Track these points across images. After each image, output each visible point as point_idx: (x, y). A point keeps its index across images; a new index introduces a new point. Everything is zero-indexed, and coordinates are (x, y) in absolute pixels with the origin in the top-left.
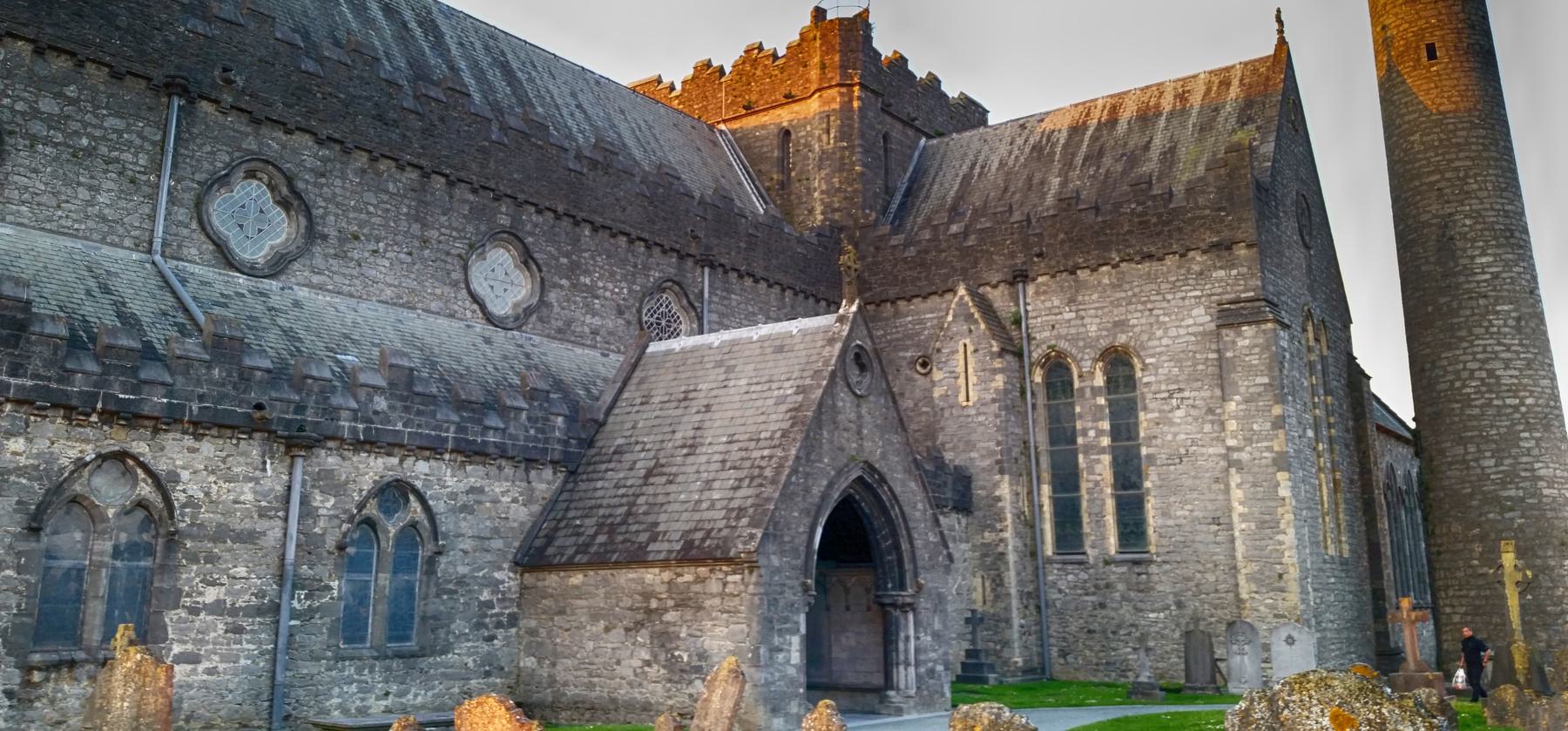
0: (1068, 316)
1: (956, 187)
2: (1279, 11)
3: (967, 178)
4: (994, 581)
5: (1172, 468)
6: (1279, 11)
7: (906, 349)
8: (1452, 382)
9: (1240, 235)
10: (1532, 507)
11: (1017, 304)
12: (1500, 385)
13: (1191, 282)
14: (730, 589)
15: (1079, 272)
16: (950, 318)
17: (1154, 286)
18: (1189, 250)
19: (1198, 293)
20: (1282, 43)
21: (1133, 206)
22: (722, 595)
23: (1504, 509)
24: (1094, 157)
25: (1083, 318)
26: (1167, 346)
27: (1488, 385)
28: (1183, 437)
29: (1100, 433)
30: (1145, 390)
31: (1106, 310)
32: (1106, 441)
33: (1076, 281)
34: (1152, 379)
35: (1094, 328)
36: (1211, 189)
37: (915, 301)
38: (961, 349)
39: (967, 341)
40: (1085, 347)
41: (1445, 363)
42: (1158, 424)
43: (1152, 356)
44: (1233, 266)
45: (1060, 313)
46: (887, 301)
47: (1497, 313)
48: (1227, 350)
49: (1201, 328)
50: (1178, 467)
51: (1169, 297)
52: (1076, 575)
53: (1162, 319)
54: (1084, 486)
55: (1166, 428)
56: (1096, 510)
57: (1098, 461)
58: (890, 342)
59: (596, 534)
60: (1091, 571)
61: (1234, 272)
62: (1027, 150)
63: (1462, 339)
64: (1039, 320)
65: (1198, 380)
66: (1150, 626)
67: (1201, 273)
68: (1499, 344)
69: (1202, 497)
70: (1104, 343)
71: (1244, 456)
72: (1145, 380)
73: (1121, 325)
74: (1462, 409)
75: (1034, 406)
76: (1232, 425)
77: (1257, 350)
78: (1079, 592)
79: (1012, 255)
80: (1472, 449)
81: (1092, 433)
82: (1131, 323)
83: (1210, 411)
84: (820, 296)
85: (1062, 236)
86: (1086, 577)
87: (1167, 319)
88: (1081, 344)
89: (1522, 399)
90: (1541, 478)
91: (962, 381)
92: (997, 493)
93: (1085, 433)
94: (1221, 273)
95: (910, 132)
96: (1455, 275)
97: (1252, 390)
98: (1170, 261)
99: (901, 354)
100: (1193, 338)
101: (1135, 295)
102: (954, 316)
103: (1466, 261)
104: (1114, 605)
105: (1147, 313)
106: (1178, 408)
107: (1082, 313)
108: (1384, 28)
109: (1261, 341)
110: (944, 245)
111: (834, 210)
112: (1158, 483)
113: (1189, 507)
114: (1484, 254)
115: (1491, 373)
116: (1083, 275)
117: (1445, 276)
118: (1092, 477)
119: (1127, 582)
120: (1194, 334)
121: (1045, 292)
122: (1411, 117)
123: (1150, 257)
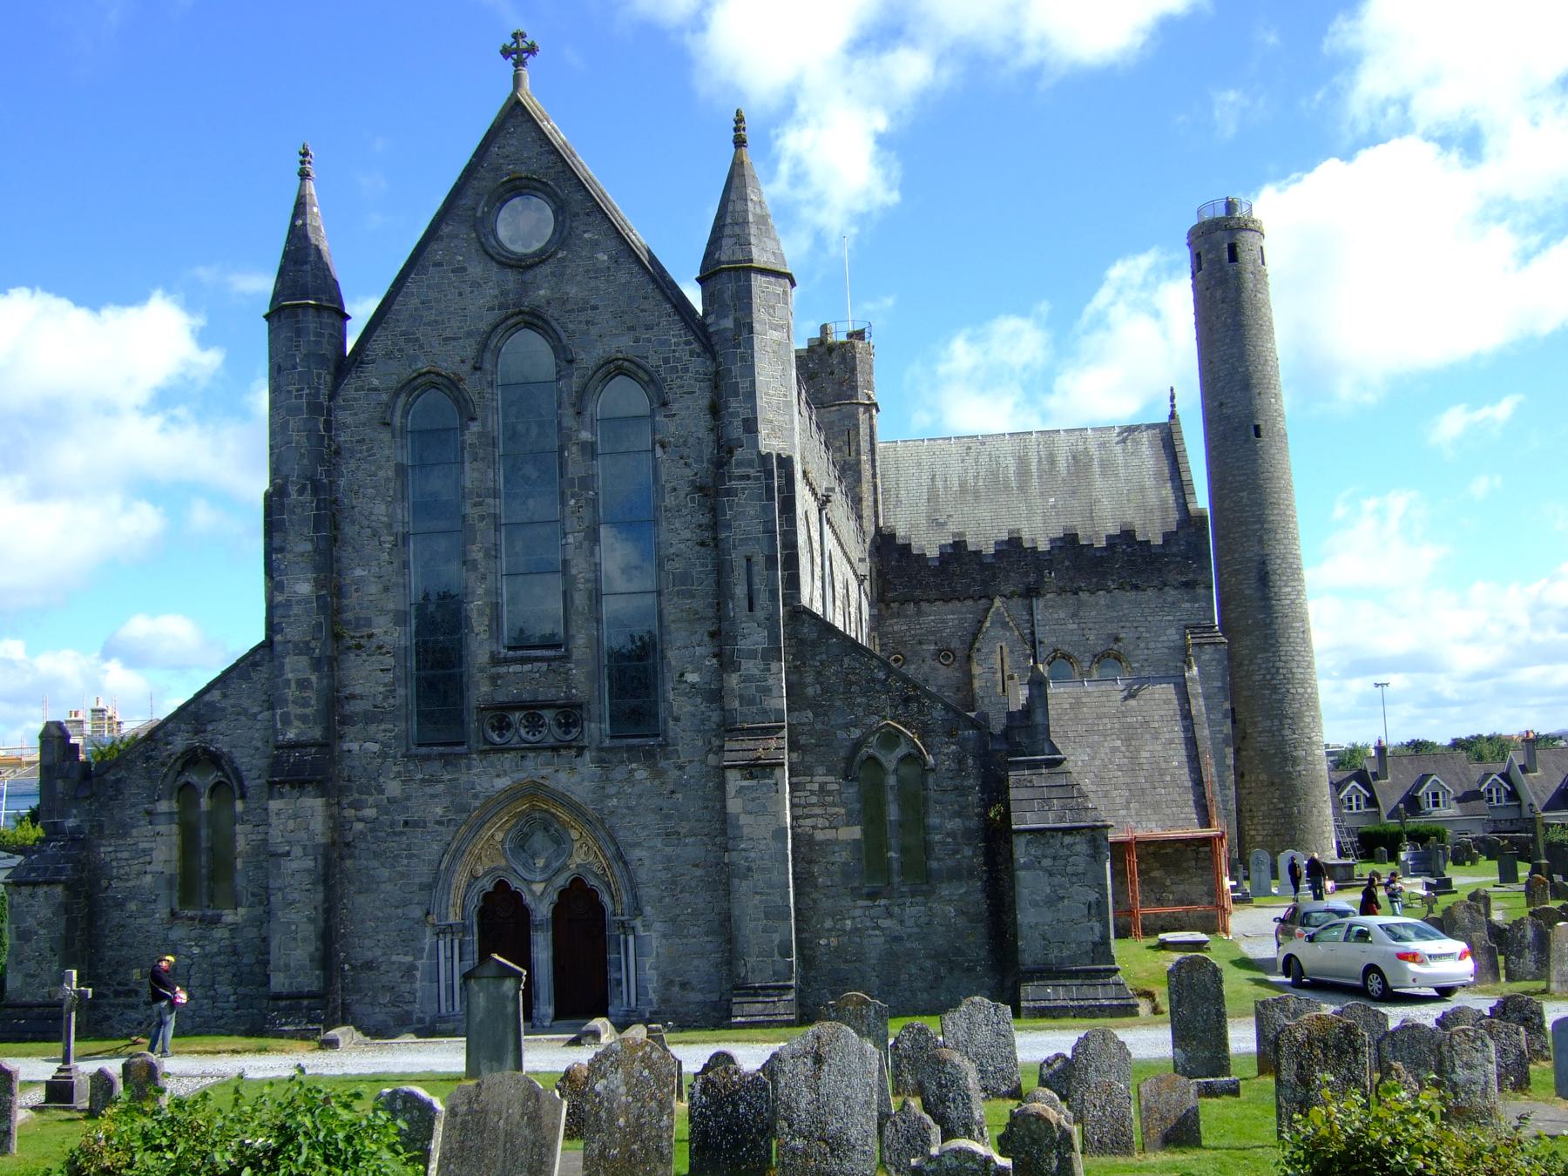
0: (1071, 627)
2: (1172, 390)
6: (1172, 390)
8: (1264, 675)
12: (1293, 678)
15: (1080, 593)
18: (1165, 585)
19: (1171, 618)
20: (1172, 416)
21: (1124, 547)
22: (1197, 860)
25: (1083, 629)
27: (1288, 679)
31: (1102, 625)
36: (1182, 542)
41: (1259, 661)
43: (1138, 662)
44: (1194, 600)
47: (1292, 628)
51: (1149, 619)
61: (1197, 605)
67: (1174, 603)
68: (1295, 650)
70: (1099, 649)
74: (1271, 695)
77: (1214, 663)
79: (1027, 574)
85: (1067, 563)
88: (1082, 649)
89: (1305, 688)
90: (1314, 743)
91: (1000, 675)
94: (1188, 605)
97: (1210, 690)
98: (1150, 592)
99: (925, 647)
101: (1124, 615)
103: (1276, 590)
105: (1133, 629)
107: (1084, 625)
108: (1221, 405)
109: (1217, 656)
114: (1286, 586)
116: (1084, 596)
120: (1169, 648)
121: (1051, 607)
122: (1242, 478)
123: (1136, 587)
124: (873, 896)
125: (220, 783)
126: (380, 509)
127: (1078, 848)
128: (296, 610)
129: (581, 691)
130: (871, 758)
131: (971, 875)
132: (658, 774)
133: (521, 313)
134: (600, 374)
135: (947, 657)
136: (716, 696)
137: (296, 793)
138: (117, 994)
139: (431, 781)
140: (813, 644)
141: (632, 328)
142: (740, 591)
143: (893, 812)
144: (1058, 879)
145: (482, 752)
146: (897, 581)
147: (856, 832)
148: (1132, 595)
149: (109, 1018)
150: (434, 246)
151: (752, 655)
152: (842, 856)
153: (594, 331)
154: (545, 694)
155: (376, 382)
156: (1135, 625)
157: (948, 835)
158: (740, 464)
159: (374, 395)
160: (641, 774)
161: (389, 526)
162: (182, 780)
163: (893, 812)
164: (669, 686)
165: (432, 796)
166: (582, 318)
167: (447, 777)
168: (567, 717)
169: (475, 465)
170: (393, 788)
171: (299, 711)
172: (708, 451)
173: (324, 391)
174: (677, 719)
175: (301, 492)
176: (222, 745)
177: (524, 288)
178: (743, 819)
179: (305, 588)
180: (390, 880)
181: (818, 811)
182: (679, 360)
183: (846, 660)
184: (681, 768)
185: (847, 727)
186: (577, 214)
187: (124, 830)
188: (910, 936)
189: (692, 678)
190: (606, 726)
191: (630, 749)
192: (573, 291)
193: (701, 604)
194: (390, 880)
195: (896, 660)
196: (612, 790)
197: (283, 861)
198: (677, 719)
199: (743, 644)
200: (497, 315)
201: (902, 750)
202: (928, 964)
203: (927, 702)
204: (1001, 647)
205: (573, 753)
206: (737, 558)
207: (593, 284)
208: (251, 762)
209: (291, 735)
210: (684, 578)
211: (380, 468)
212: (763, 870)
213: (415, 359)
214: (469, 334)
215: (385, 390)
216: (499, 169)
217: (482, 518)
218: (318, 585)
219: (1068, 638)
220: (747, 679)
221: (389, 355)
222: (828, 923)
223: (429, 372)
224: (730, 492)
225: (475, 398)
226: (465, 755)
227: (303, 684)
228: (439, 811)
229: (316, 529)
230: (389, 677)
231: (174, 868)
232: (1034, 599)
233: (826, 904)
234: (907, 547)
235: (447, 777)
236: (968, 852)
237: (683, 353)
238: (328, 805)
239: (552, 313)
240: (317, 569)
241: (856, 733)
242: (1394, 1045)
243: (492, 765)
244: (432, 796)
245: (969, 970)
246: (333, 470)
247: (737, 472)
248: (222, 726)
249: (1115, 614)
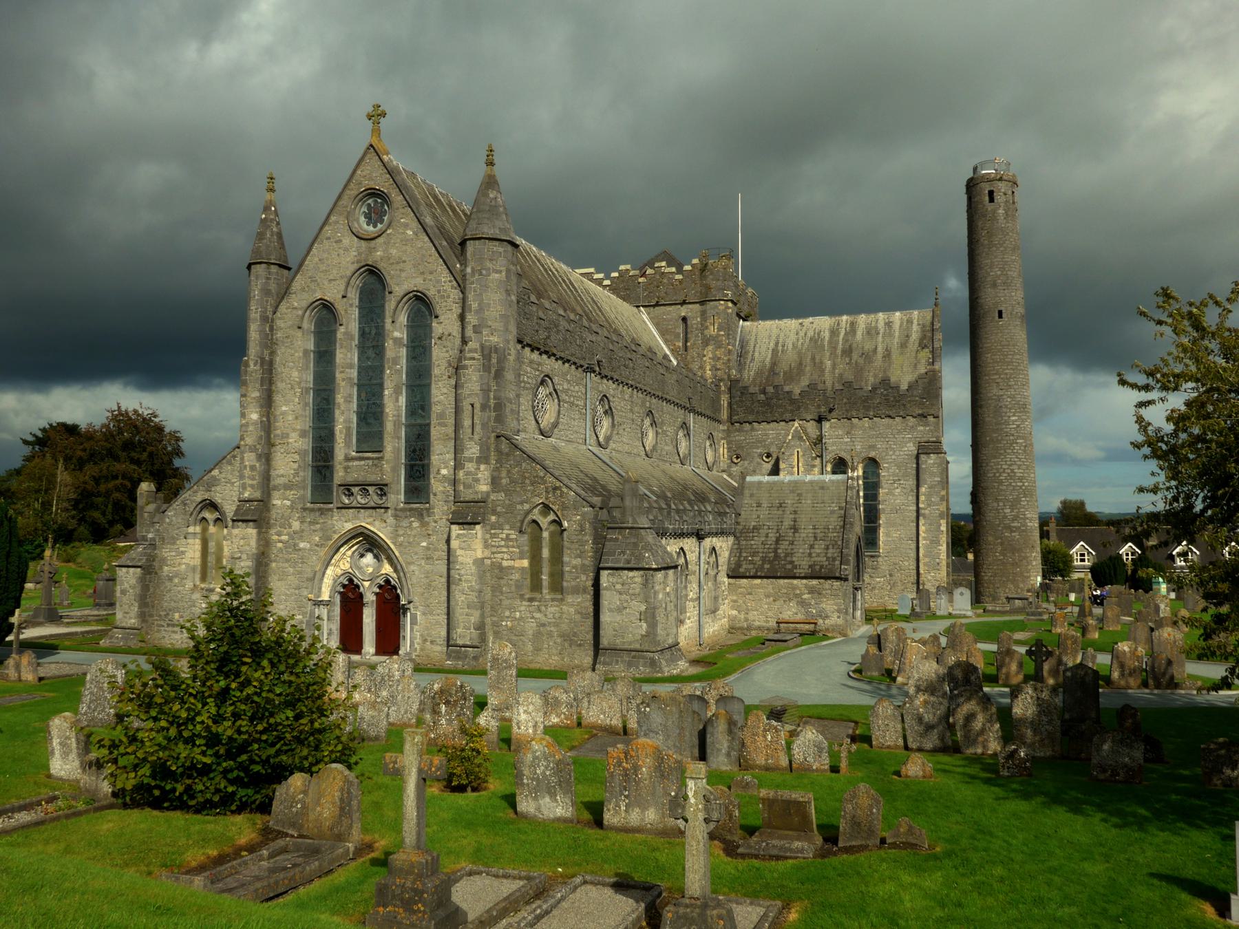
1: (770, 356)
3: (775, 351)
7: (758, 448)
9: (932, 412)
10: (1023, 531)
14: (835, 587)
16: (790, 437)
23: (1012, 531)
24: (848, 352)
44: (927, 425)
58: (748, 443)
59: (763, 564)
62: (807, 341)
63: (1001, 454)
70: (864, 455)
71: (927, 512)
73: (873, 447)
76: (922, 498)
79: (819, 406)
80: (1001, 504)
83: (912, 490)
94: (922, 428)
96: (1000, 424)
98: (898, 419)
110: (781, 397)
111: (717, 369)
115: (1012, 471)
116: (855, 421)
117: (996, 424)
123: (890, 417)
124: (531, 600)
125: (218, 519)
126: (295, 374)
127: (636, 580)
128: (251, 428)
129: (387, 478)
130: (534, 521)
131: (585, 591)
132: (424, 524)
133: (367, 265)
134: (405, 299)
135: (767, 457)
136: (455, 482)
137: (244, 525)
138: (168, 625)
139: (312, 523)
140: (507, 455)
141: (423, 273)
142: (467, 423)
143: (546, 553)
144: (624, 596)
145: (338, 508)
146: (739, 409)
147: (525, 563)
148: (887, 420)
149: (164, 637)
150: (327, 228)
151: (471, 460)
152: (516, 576)
153: (403, 275)
154: (372, 478)
155: (296, 304)
157: (573, 568)
158: (470, 351)
159: (295, 312)
160: (416, 524)
161: (300, 383)
162: (201, 516)
163: (546, 553)
164: (431, 476)
165: (314, 531)
166: (398, 268)
167: (321, 521)
168: (381, 490)
169: (342, 351)
170: (296, 525)
171: (251, 482)
172: (458, 341)
173: (270, 309)
174: (435, 495)
175: (255, 365)
176: (218, 499)
177: (371, 250)
178: (459, 552)
179: (255, 416)
180: (293, 574)
181: (504, 550)
182: (445, 291)
183: (524, 465)
184: (436, 522)
185: (522, 503)
186: (398, 209)
187: (173, 541)
188: (549, 623)
189: (444, 472)
190: (402, 497)
191: (411, 510)
192: (394, 252)
193: (451, 430)
194: (293, 574)
195: (737, 458)
196: (401, 532)
197: (237, 561)
198: (435, 495)
199: (467, 454)
200: (356, 266)
201: (552, 517)
202: (559, 640)
203: (565, 490)
205: (383, 510)
206: (466, 406)
207: (404, 248)
208: (230, 509)
209: (246, 495)
210: (441, 416)
211: (296, 351)
212: (467, 581)
213: (315, 291)
214: (342, 277)
215: (301, 309)
216: (360, 184)
217: (343, 380)
218: (262, 416)
219: (844, 447)
220: (468, 473)
221: (303, 290)
222: (507, 613)
223: (321, 299)
224: (465, 367)
225: (343, 313)
226: (331, 510)
227: (253, 468)
228: (317, 538)
229: (262, 385)
230: (295, 466)
231: (197, 562)
233: (506, 602)
235: (321, 521)
236: (583, 578)
237: (448, 287)
238: (259, 533)
239: (382, 266)
240: (261, 406)
241: (527, 506)
242: (589, 702)
243: (343, 516)
244: (314, 531)
245: (580, 645)
246: (273, 353)
247: (468, 355)
248: (218, 488)
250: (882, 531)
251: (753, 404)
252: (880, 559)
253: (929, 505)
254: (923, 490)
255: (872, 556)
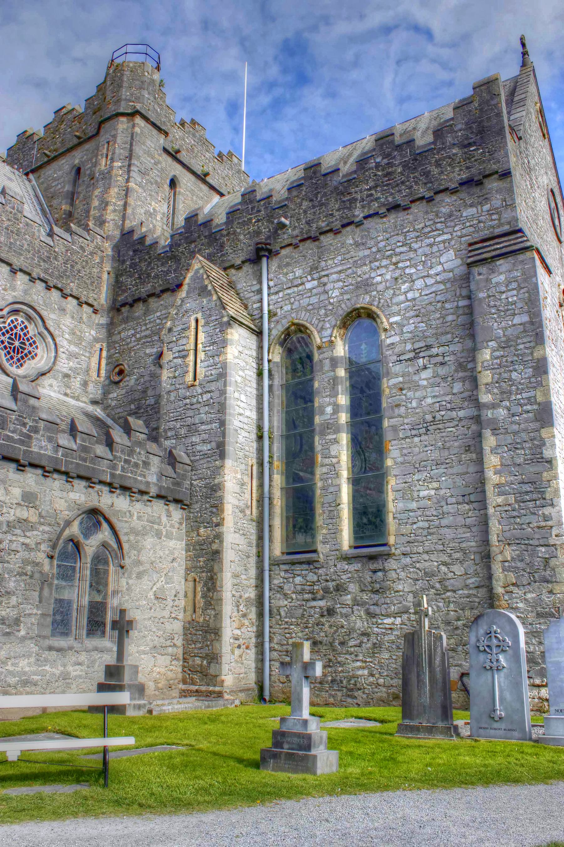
0: (309, 286)
4: (205, 584)
5: (416, 439)
11: (260, 282)
13: (439, 226)
15: (322, 238)
17: (401, 238)
19: (446, 237)
21: (378, 160)
25: (325, 285)
26: (414, 299)
28: (429, 401)
29: (337, 409)
30: (390, 352)
31: (350, 271)
32: (344, 418)
33: (319, 247)
34: (396, 339)
35: (336, 293)
37: (165, 295)
38: (193, 324)
39: (199, 316)
40: (326, 315)
42: (401, 389)
45: (303, 284)
46: (139, 300)
48: (479, 289)
49: (451, 275)
50: (424, 438)
52: (304, 577)
53: (408, 271)
54: (319, 471)
55: (410, 394)
56: (330, 498)
57: (336, 441)
58: (139, 340)
60: (320, 571)
61: (486, 207)
64: (281, 294)
65: (448, 333)
66: (384, 634)
69: (450, 471)
70: (345, 308)
72: (389, 341)
75: (271, 387)
76: (486, 377)
77: (514, 285)
78: (307, 596)
81: (329, 410)
82: (375, 281)
84: (68, 291)
86: (315, 578)
87: (413, 270)
88: (322, 312)
91: (191, 357)
92: (216, 481)
93: (322, 413)
94: (473, 211)
95: (204, 188)
97: (509, 332)
98: (417, 209)
100: (442, 287)
102: (188, 293)
104: (344, 611)
106: (425, 368)
107: (325, 280)
112: (400, 460)
113: (435, 485)
116: (326, 240)
118: (327, 461)
119: (360, 582)
121: (288, 265)
123: (395, 207)
148: (392, 218)
156: (394, 260)
204: (197, 321)
232: (264, 260)
234: (143, 239)
249: (367, 252)
250: (392, 483)
251: (150, 263)
252: (392, 564)
253: (505, 394)
254: (486, 355)
255: (372, 558)
